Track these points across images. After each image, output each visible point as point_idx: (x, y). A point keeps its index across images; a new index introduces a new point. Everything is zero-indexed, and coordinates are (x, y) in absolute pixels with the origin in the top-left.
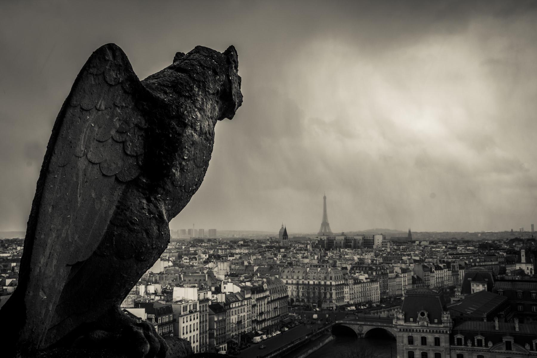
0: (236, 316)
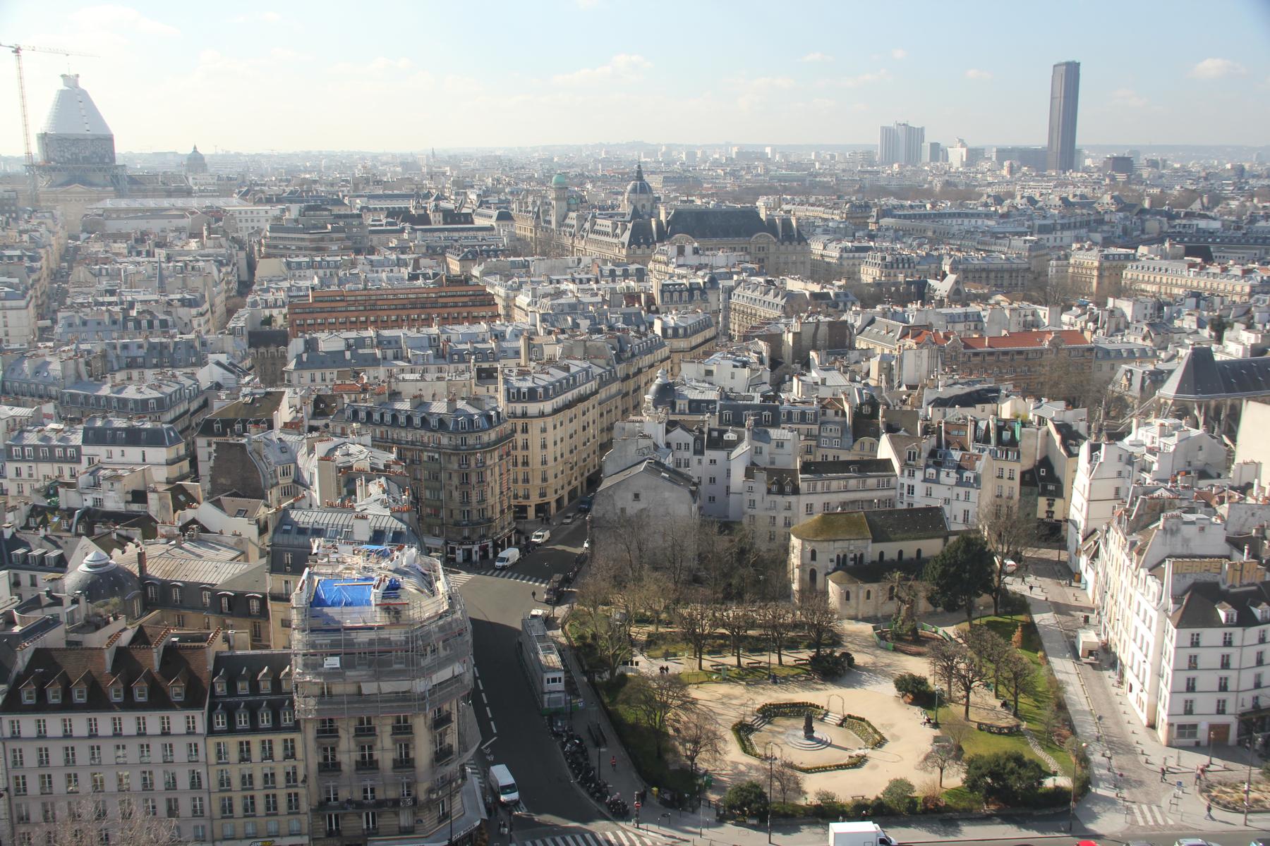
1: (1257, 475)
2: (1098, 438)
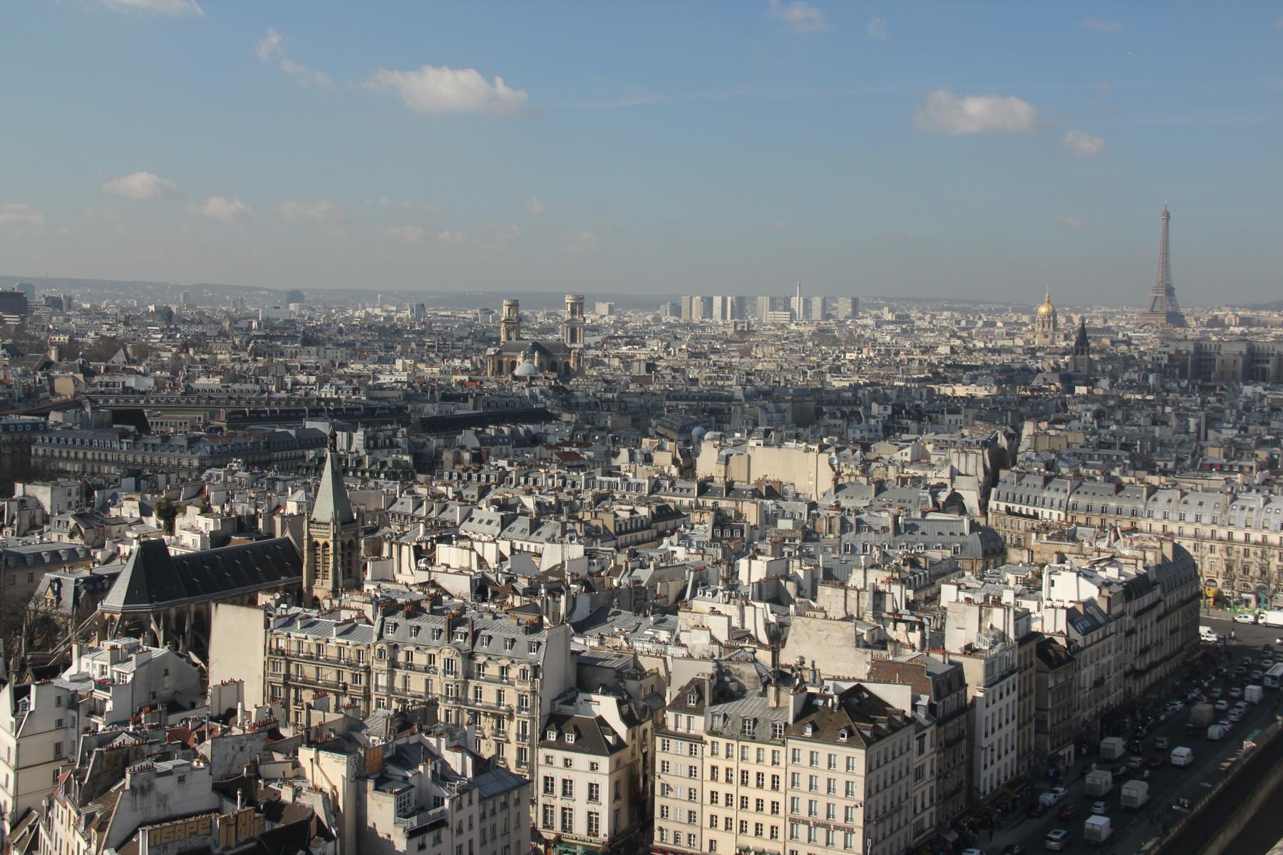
0: (1092, 667)
1: (240, 698)
2: (20, 677)
